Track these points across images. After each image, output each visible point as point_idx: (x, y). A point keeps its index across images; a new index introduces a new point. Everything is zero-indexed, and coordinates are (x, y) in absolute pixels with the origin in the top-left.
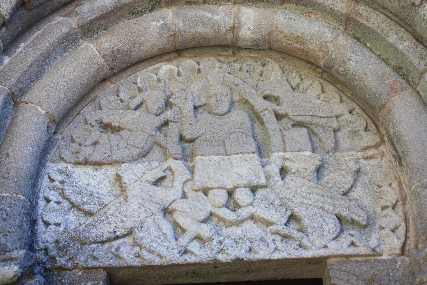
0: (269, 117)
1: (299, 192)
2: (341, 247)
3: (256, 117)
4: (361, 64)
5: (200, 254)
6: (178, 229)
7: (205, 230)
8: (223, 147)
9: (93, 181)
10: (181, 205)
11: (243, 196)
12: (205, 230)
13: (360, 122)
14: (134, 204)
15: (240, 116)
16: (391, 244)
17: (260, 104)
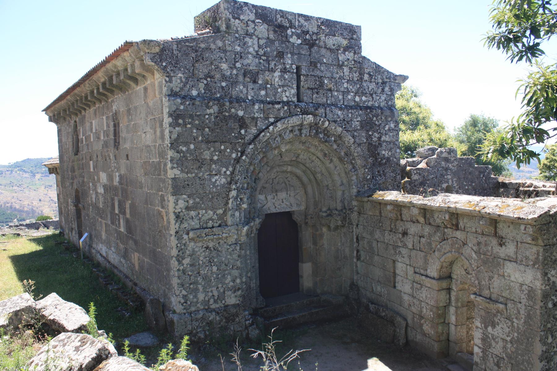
0: (288, 184)
1: (292, 200)
2: (297, 209)
3: (285, 183)
4: (305, 179)
5: (279, 211)
6: (276, 207)
7: (279, 207)
8: (281, 190)
9: (262, 197)
10: (276, 203)
11: (284, 201)
12: (279, 207)
13: (301, 186)
14: (269, 203)
15: (283, 185)
16: (303, 208)
17: (287, 183)
